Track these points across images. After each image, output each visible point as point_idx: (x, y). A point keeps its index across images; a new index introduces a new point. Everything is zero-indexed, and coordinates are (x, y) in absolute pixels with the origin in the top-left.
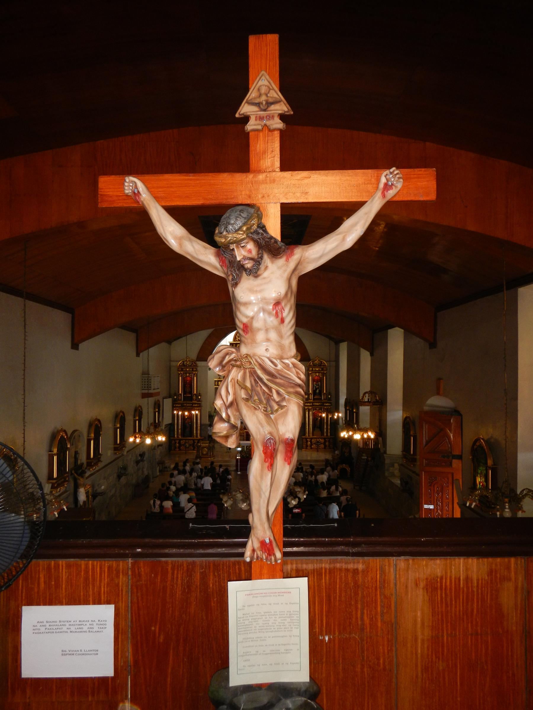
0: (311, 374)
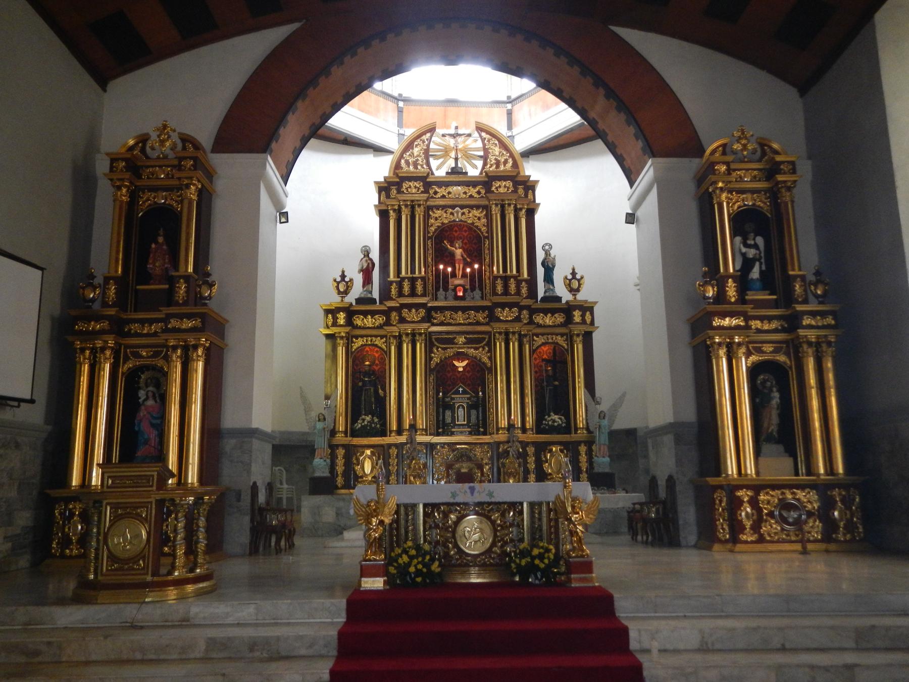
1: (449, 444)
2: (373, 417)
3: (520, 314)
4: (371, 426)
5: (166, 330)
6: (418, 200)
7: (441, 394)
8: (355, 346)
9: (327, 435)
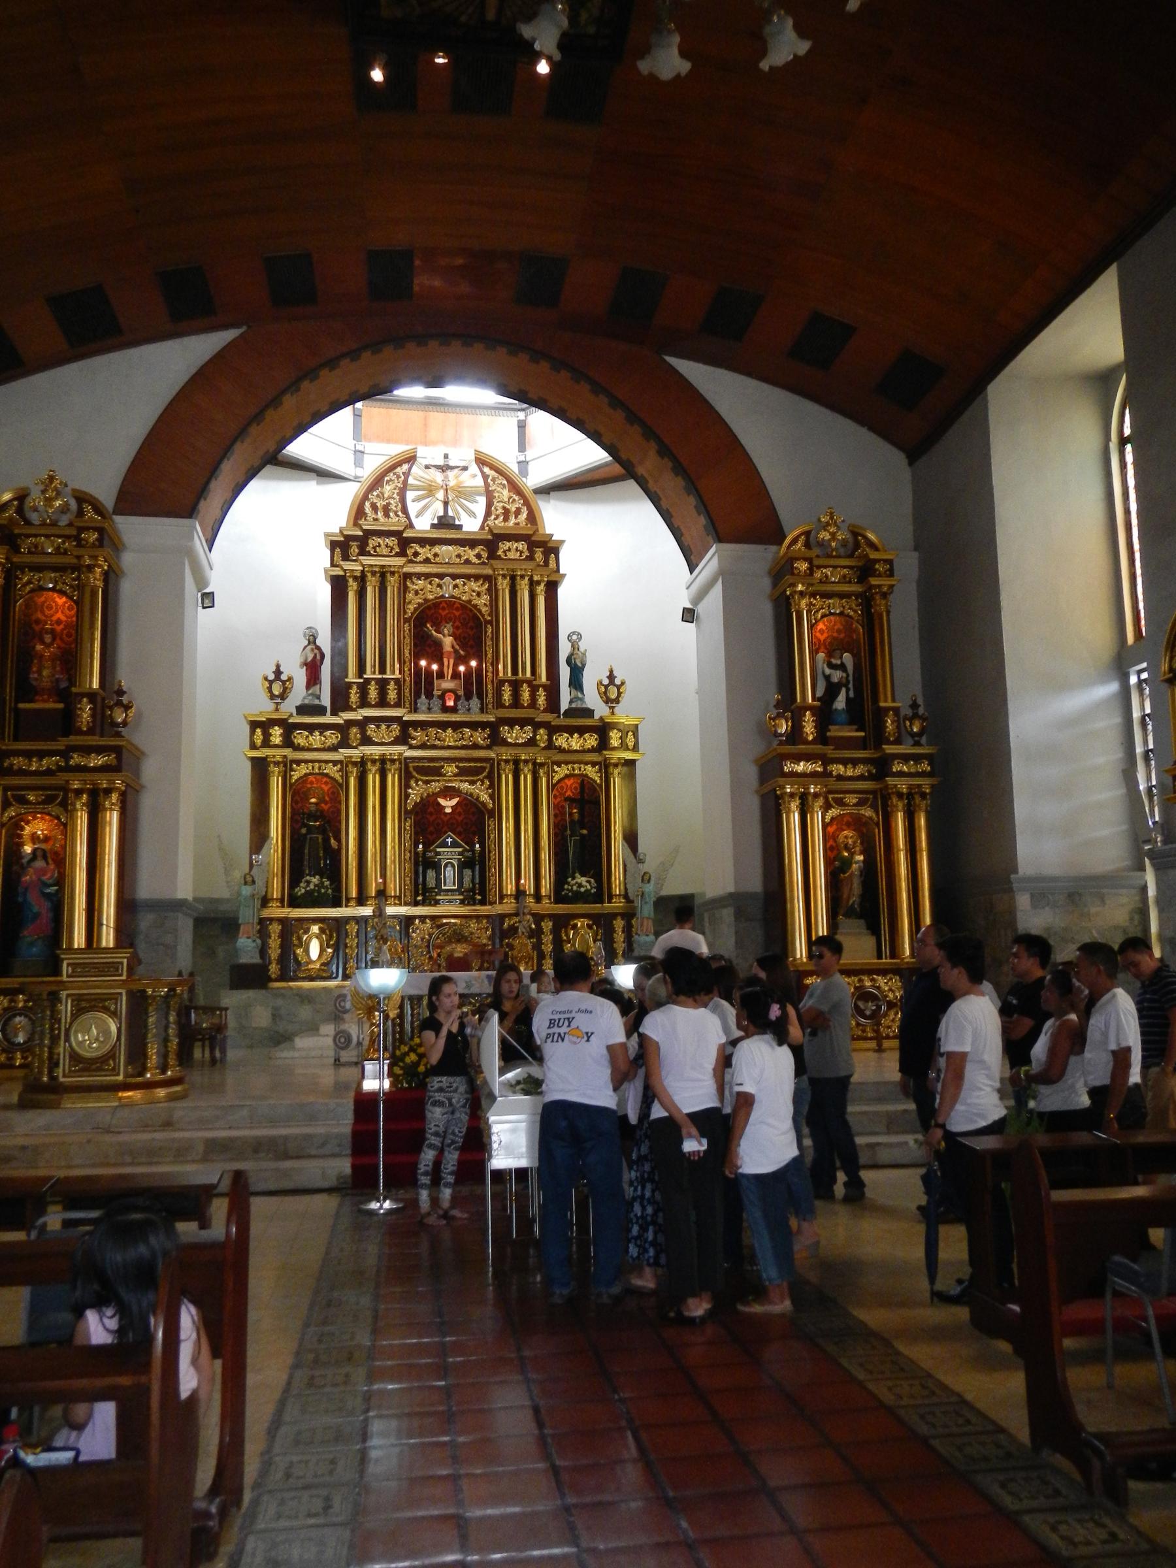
0: (802, 593)
1: (433, 918)
2: (322, 878)
3: (535, 735)
4: (319, 892)
5: (68, 769)
6: (390, 566)
7: (421, 846)
8: (296, 776)
9: (258, 903)
